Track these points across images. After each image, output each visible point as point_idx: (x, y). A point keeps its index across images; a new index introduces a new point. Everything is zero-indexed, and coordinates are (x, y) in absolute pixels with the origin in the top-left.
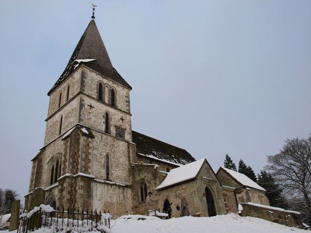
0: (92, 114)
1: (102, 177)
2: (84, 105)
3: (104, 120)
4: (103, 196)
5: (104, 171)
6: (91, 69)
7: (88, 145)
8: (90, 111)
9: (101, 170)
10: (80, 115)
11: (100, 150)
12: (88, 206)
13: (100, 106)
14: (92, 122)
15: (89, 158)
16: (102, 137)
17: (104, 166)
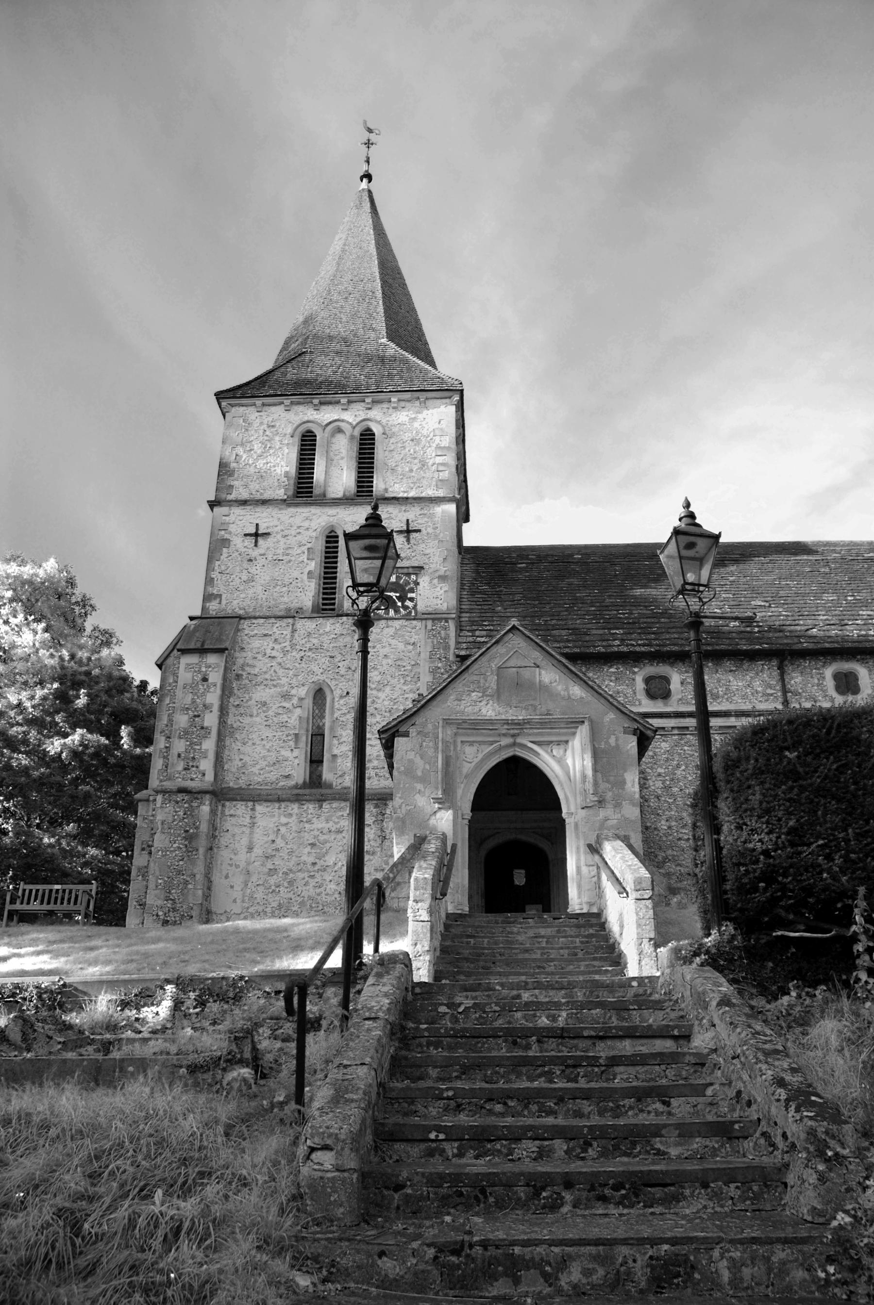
0: (261, 561)
1: (288, 777)
2: (225, 542)
3: (314, 565)
4: (280, 843)
5: (296, 752)
6: (259, 402)
7: (205, 680)
8: (255, 553)
9: (286, 753)
10: (209, 581)
11: (284, 681)
12: (186, 883)
13: (298, 521)
14: (260, 589)
15: (206, 724)
16: (294, 631)
17: (296, 735)
